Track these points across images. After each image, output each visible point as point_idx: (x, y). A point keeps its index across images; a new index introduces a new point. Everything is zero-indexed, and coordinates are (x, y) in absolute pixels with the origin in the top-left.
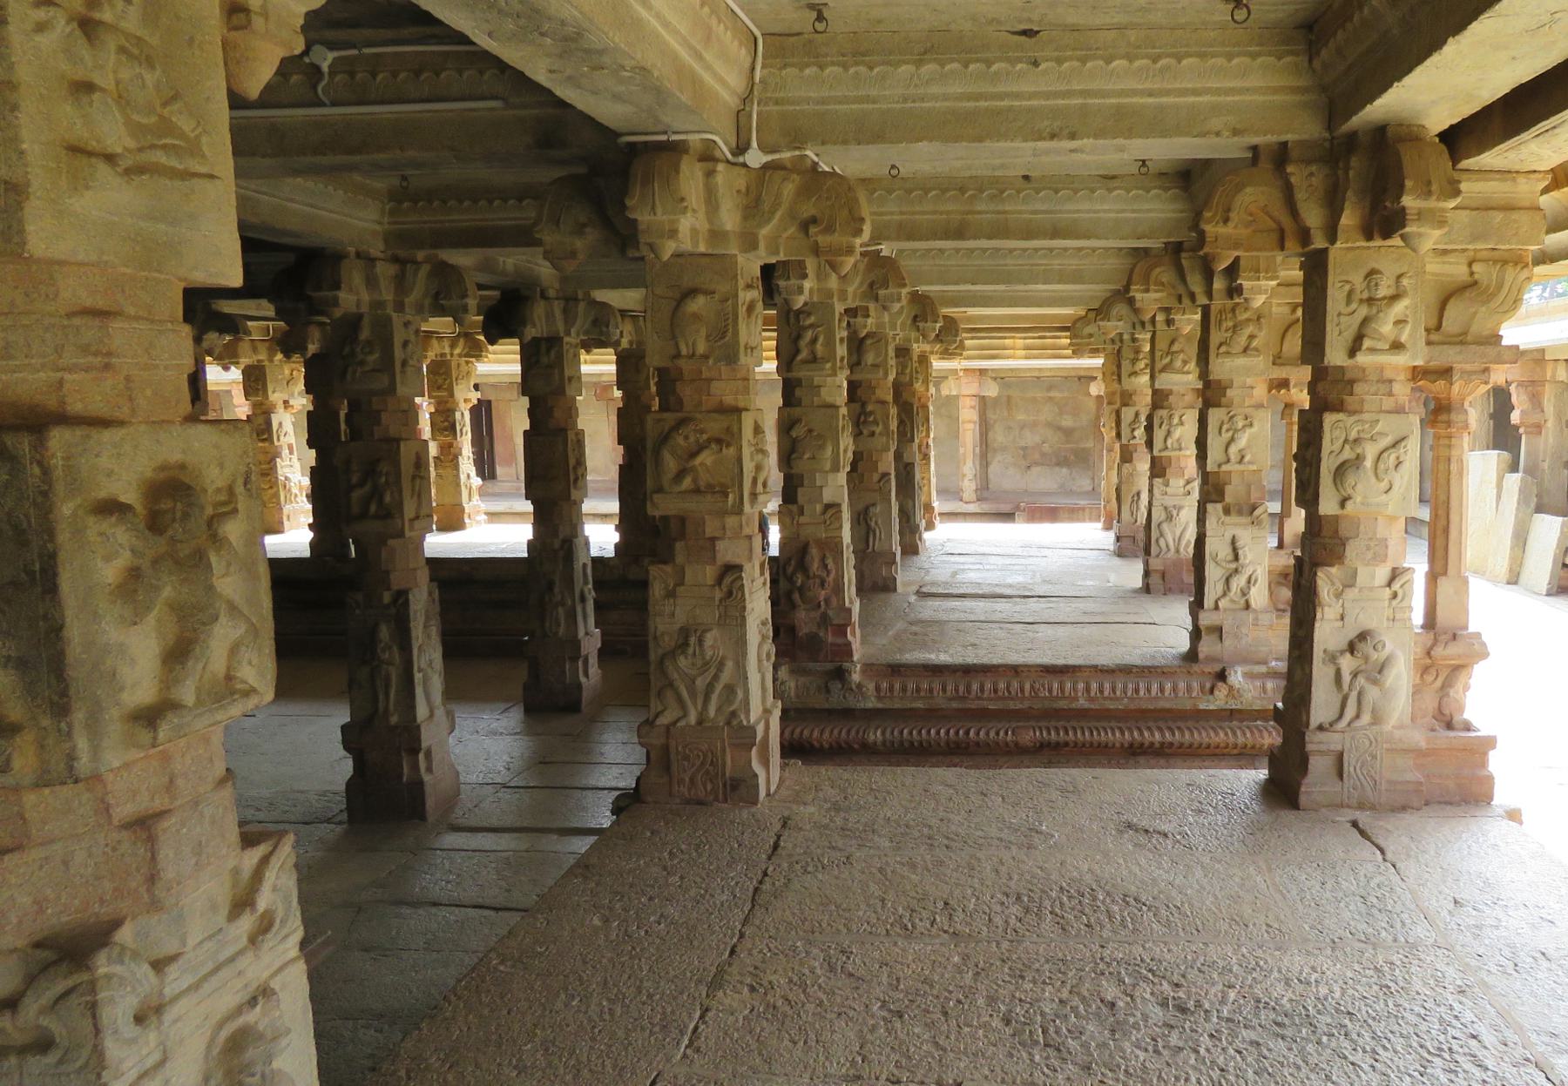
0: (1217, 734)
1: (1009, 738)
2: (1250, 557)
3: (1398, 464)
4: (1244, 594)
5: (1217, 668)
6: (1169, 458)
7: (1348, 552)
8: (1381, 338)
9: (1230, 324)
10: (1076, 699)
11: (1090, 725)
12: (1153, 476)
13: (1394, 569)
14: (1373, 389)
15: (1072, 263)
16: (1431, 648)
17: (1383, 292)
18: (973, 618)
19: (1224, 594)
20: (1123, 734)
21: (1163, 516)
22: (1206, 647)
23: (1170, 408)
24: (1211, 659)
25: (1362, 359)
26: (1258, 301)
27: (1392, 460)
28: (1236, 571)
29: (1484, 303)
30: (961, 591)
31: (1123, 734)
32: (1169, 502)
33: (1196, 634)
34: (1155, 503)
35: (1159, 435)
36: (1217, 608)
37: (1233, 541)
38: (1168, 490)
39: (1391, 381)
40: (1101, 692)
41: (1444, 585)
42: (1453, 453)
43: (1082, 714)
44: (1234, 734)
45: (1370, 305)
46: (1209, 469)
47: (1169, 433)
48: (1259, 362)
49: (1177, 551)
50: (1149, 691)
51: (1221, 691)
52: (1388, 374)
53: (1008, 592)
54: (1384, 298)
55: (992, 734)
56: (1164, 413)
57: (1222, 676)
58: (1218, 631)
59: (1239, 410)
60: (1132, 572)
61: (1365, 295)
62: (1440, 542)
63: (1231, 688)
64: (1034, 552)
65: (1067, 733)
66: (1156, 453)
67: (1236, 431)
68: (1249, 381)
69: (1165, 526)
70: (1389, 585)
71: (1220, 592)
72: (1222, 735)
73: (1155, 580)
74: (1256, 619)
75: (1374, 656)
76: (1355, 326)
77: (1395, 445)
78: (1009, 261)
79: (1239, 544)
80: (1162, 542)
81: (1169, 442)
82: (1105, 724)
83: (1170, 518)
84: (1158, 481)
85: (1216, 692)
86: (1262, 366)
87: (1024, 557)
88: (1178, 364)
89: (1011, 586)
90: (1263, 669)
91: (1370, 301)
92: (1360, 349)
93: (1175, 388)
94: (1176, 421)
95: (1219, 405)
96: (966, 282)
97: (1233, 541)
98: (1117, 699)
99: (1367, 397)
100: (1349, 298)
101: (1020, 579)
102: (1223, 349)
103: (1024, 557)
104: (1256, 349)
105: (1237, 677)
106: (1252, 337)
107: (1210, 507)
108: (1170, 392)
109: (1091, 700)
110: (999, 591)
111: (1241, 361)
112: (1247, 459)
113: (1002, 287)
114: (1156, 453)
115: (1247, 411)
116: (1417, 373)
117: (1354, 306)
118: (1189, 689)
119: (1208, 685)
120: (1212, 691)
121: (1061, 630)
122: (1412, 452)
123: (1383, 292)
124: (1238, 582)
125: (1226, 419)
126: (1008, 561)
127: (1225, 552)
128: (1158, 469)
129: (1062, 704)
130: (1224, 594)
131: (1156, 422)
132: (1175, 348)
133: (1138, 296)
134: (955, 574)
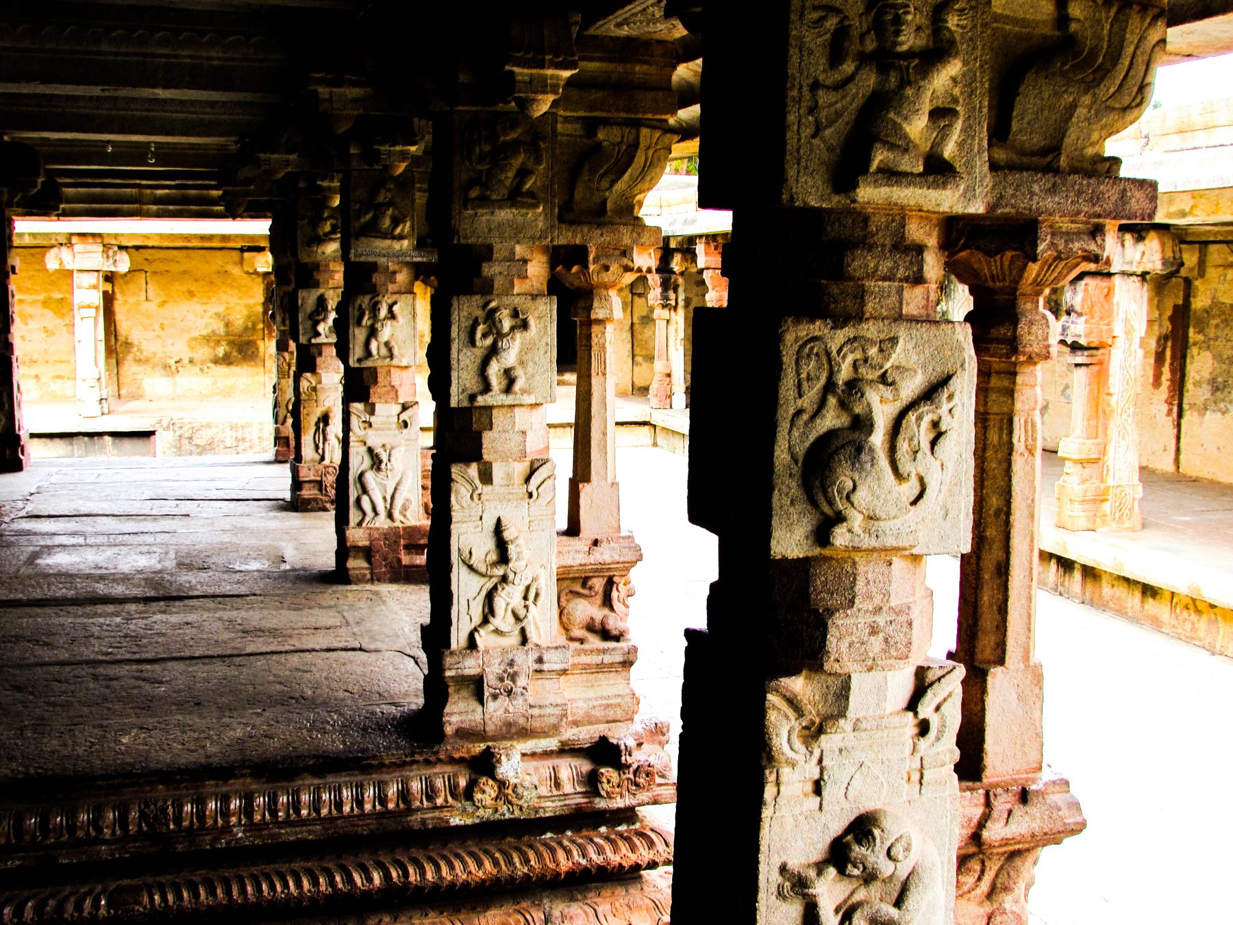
0: (480, 864)
1: (103, 912)
2: (527, 554)
3: (938, 436)
4: (517, 618)
5: (479, 747)
6: (373, 372)
7: (832, 642)
8: (906, 147)
9: (487, 148)
10: (227, 828)
11: (254, 870)
12: (347, 400)
13: (921, 672)
14: (885, 266)
15: (215, 56)
16: (981, 825)
17: (908, 40)
18: (47, 655)
19: (485, 621)
20: (315, 883)
21: (367, 462)
22: (459, 712)
23: (374, 291)
24: (465, 734)
25: (868, 193)
26: (543, 105)
27: (925, 436)
28: (504, 579)
29: (1091, 86)
30: (38, 594)
31: (315, 883)
32: (374, 439)
33: (436, 688)
34: (352, 438)
35: (359, 335)
36: (472, 644)
37: (498, 529)
38: (373, 419)
39: (920, 249)
40: (274, 813)
41: (999, 682)
42: (1018, 406)
43: (239, 856)
44: (510, 862)
45: (883, 70)
46: (454, 403)
47: (373, 333)
48: (537, 217)
49: (390, 516)
50: (360, 802)
51: (487, 793)
52: (916, 231)
53: (119, 590)
54: (910, 54)
55: (70, 907)
56: (365, 301)
57: (485, 765)
58: (476, 687)
59: (506, 300)
60: (315, 540)
61: (870, 45)
62: (987, 597)
63: (502, 784)
64: (168, 507)
65: (212, 892)
66: (352, 363)
67: (500, 335)
68: (519, 250)
69: (370, 478)
70: (912, 706)
71: (477, 619)
72: (488, 865)
73: (356, 564)
74: (540, 660)
75: (886, 868)
76: (849, 116)
77: (930, 394)
78: (104, 47)
79: (507, 535)
80: (365, 502)
81: (374, 345)
82: (284, 867)
83: (376, 463)
84: (357, 407)
85: (478, 796)
86: (541, 224)
87: (155, 517)
88: (387, 223)
89: (125, 579)
90: (552, 743)
91: (884, 59)
92: (864, 170)
93: (382, 261)
94: (383, 312)
95: (470, 292)
96: (29, 79)
97: (498, 529)
98: (303, 822)
99: (870, 284)
100: (835, 57)
101: (143, 562)
102: (474, 193)
103: (155, 517)
104: (531, 194)
105: (511, 766)
106: (523, 173)
107: (455, 470)
108: (374, 267)
109: (251, 827)
110: (101, 588)
111: (504, 215)
112: (517, 387)
113: (96, 91)
114: (352, 363)
115: (517, 300)
116: (956, 231)
117: (848, 67)
118: (431, 793)
119: (463, 782)
120: (468, 794)
121: (201, 671)
122: (960, 410)
123: (908, 40)
124: (508, 599)
125: (480, 313)
126: (131, 526)
127: (483, 549)
128: (359, 387)
129: (206, 843)
130: (485, 621)
131: (353, 313)
132: (381, 199)
133: (323, 91)
134: (36, 555)
